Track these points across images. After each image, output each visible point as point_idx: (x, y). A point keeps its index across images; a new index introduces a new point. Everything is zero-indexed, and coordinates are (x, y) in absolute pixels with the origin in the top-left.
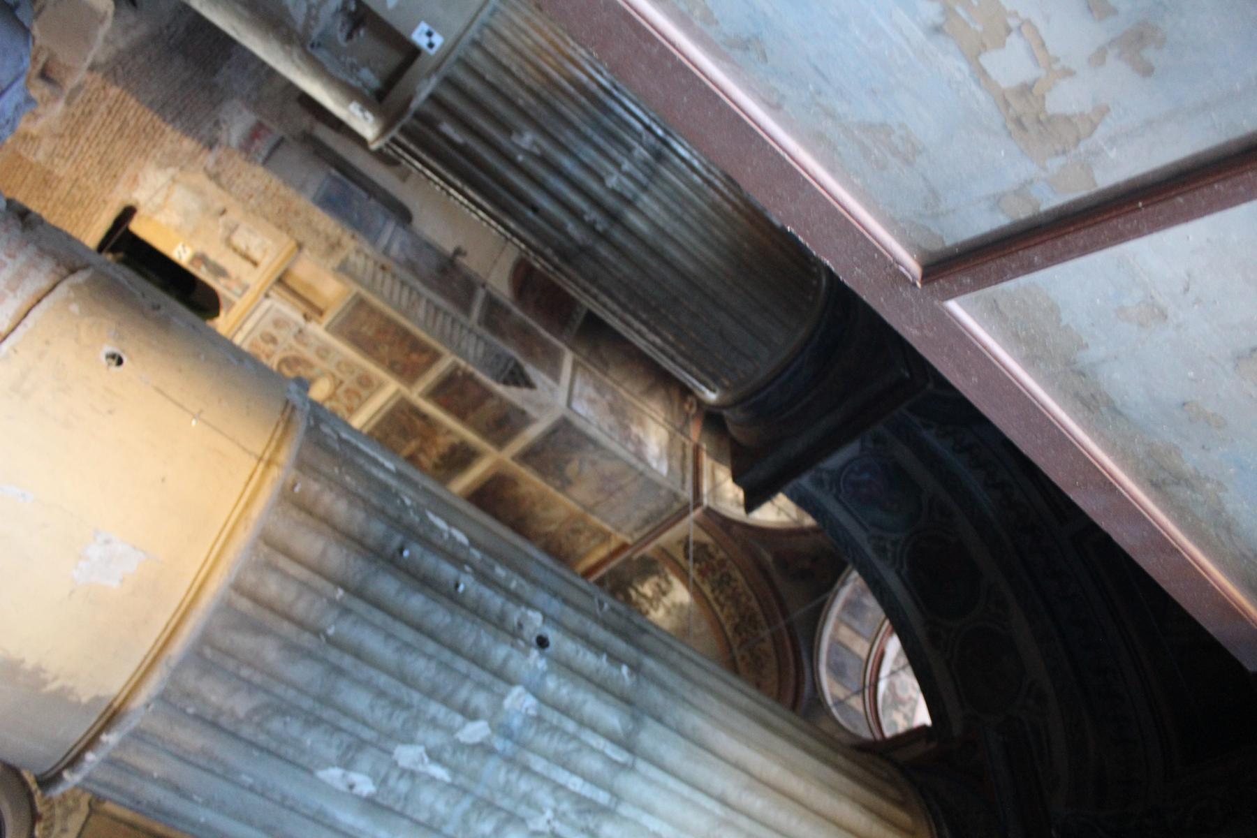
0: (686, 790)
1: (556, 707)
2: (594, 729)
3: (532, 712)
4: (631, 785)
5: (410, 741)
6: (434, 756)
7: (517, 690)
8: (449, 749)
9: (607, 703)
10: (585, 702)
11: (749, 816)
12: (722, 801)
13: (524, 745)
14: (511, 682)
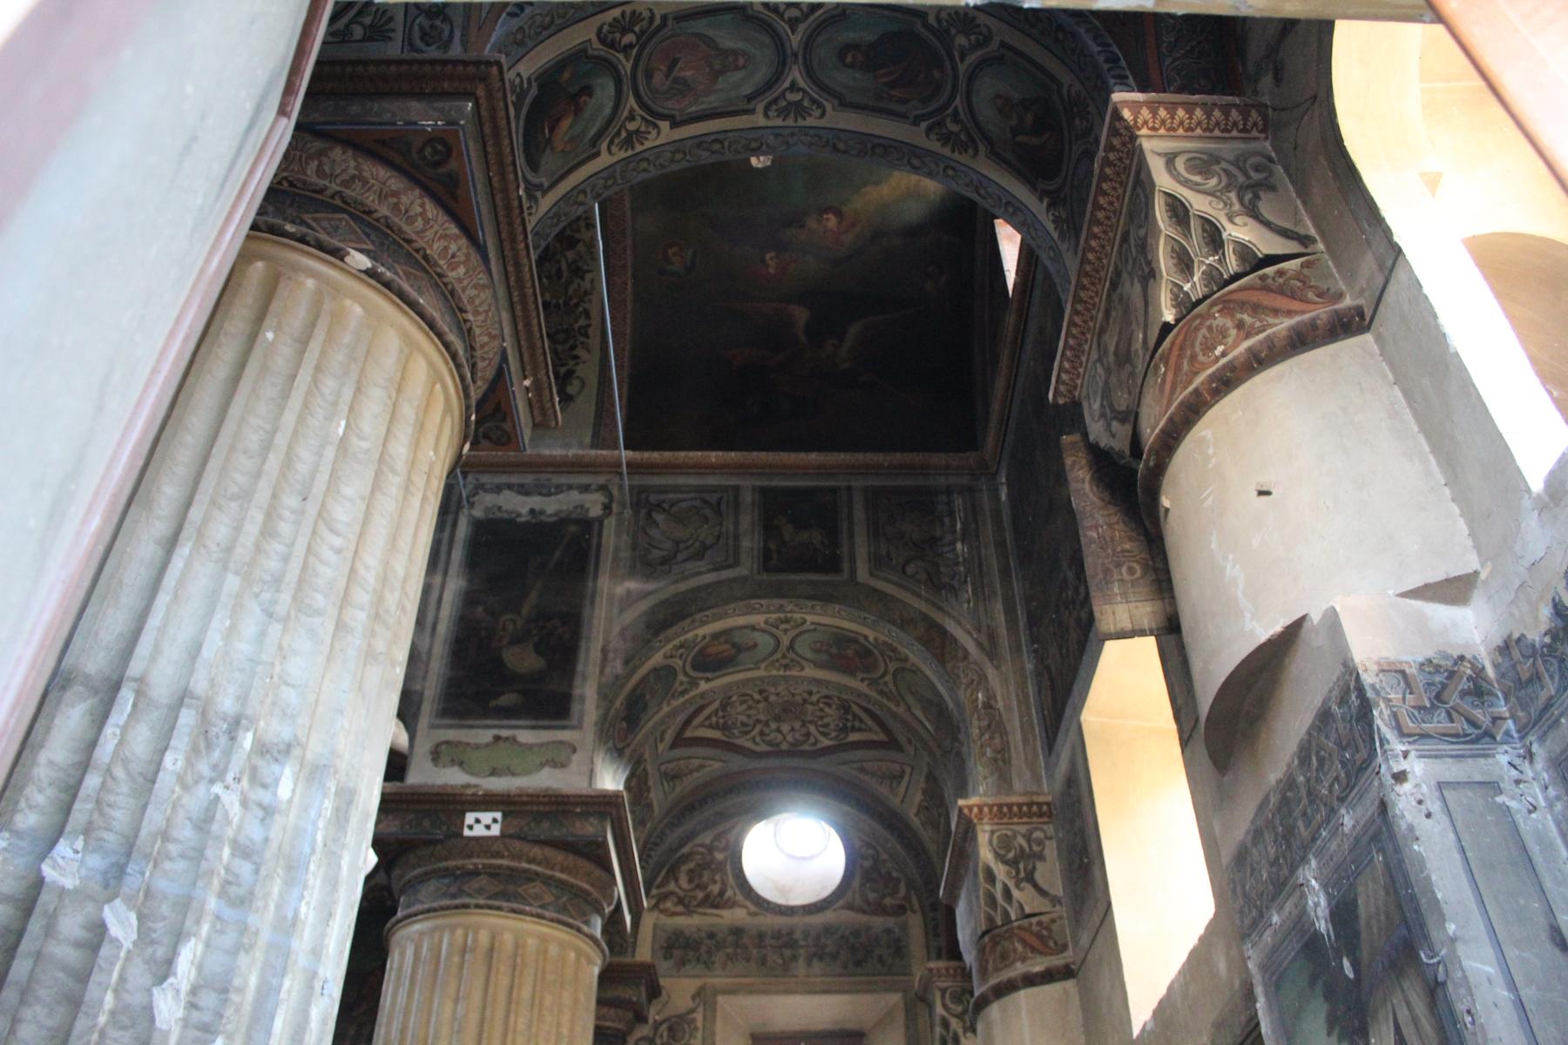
0: (163, 599)
1: (67, 810)
2: (92, 744)
3: (79, 844)
4: (162, 683)
5: (149, 1011)
6: (164, 970)
7: (47, 871)
8: (150, 950)
9: (48, 730)
10: (50, 763)
11: (188, 504)
12: (171, 544)
13: (129, 847)
14: (39, 883)
